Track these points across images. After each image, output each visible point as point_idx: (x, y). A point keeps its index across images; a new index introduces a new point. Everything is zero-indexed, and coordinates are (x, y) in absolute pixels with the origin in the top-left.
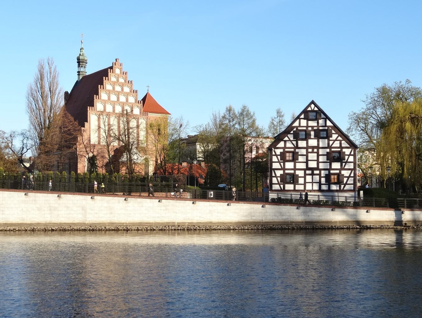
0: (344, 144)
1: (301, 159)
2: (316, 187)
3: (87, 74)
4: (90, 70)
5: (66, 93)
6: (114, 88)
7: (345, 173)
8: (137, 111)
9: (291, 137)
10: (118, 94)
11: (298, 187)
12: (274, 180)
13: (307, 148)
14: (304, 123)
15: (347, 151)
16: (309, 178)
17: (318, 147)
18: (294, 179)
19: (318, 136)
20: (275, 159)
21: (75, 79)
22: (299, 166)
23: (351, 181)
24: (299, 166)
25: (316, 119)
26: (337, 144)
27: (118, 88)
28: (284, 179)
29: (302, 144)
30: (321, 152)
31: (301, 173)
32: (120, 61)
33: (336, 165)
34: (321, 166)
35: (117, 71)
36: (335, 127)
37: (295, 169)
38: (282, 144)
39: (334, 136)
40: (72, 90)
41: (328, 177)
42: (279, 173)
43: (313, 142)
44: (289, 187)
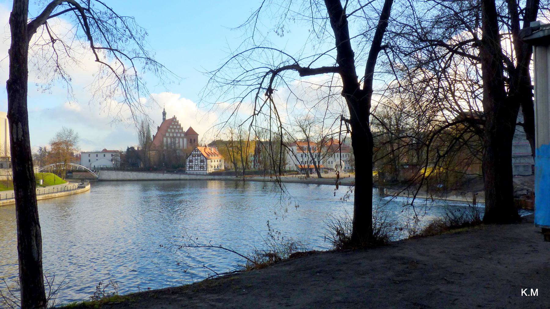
0: (204, 158)
1: (194, 162)
2: (197, 170)
3: (166, 119)
4: (168, 117)
5: (158, 127)
6: (173, 127)
7: (204, 166)
8: (183, 135)
9: (191, 156)
10: (175, 129)
11: (193, 170)
12: (187, 168)
13: (195, 159)
14: (194, 152)
15: (205, 160)
16: (196, 167)
17: (198, 159)
18: (192, 168)
19: (198, 156)
20: (187, 162)
21: (162, 121)
22: (193, 164)
23: (206, 168)
24: (193, 164)
25: (198, 151)
26: (202, 158)
27: (175, 127)
28: (190, 167)
29: (194, 158)
30: (199, 160)
31: (194, 166)
32: (176, 116)
33: (202, 164)
34: (199, 164)
35: (174, 120)
36: (202, 154)
37: (192, 165)
38: (189, 158)
39: (202, 156)
40: (161, 126)
41: (200, 167)
42: (188, 166)
43: (196, 158)
44: (191, 169)
